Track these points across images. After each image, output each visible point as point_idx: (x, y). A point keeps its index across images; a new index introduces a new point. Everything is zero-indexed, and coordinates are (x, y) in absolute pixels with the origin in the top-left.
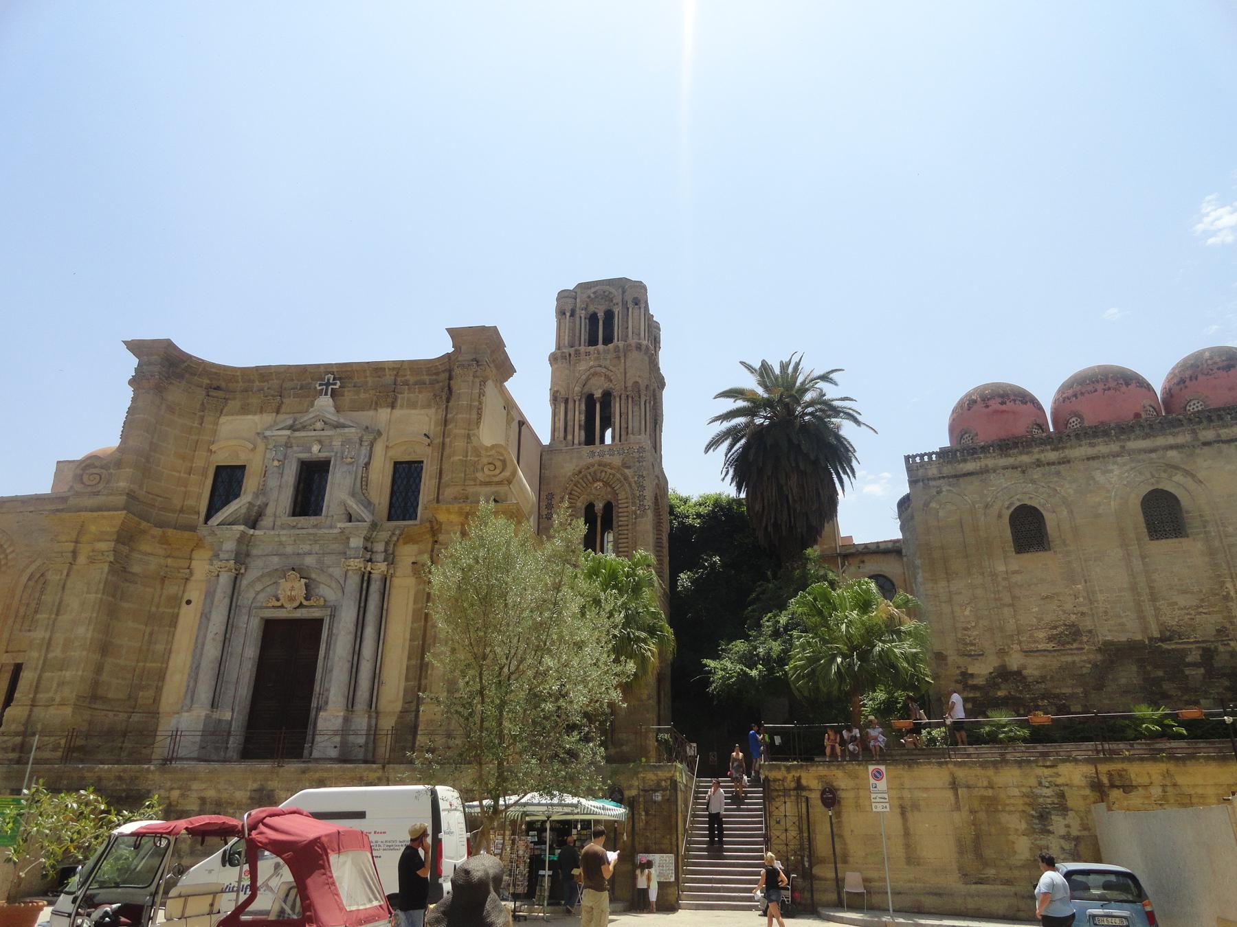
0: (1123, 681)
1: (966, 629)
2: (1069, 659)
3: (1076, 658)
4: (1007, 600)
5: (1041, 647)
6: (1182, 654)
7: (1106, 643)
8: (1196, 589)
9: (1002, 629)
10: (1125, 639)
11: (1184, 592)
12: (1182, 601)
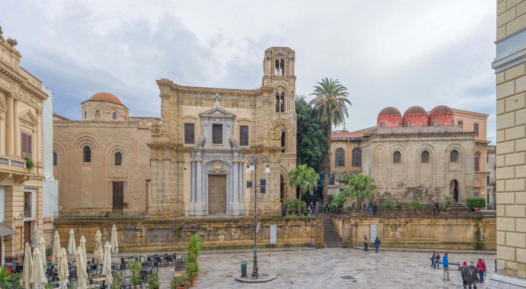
0: (410, 196)
1: (380, 182)
2: (400, 191)
3: (402, 190)
4: (390, 176)
5: (395, 187)
6: (422, 191)
7: (408, 188)
8: (428, 176)
9: (388, 183)
10: (412, 187)
11: (425, 176)
12: (425, 178)
